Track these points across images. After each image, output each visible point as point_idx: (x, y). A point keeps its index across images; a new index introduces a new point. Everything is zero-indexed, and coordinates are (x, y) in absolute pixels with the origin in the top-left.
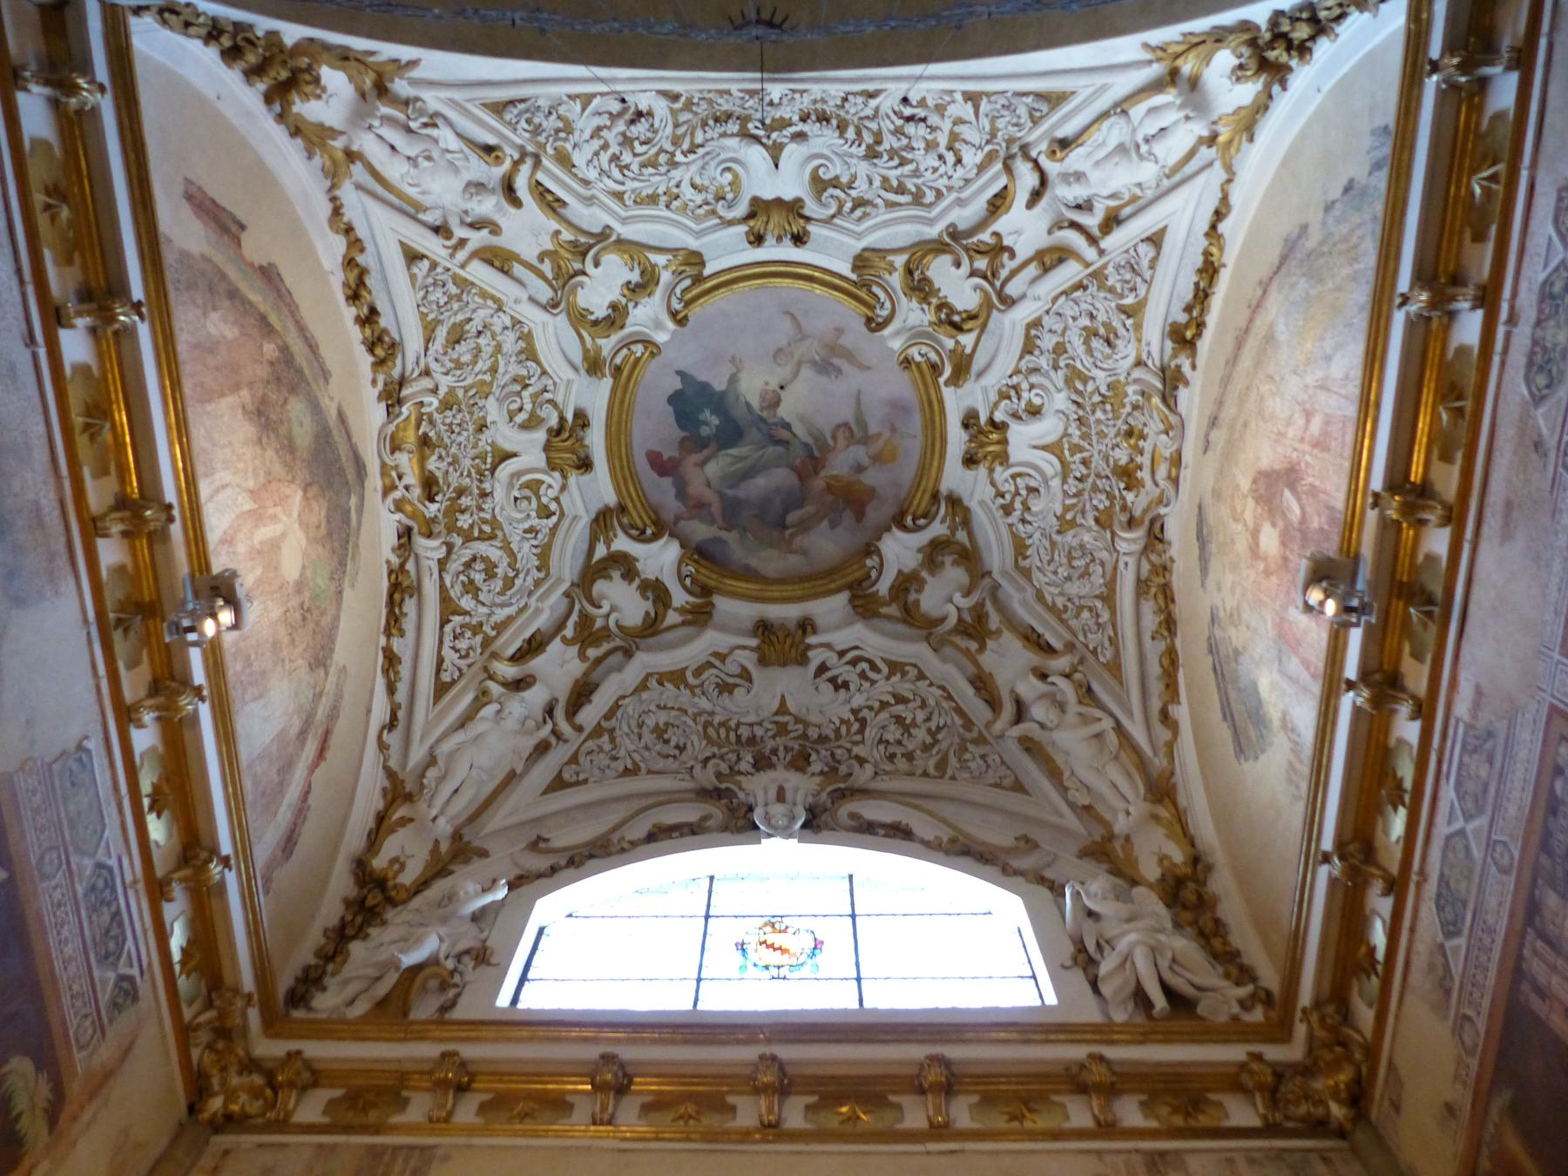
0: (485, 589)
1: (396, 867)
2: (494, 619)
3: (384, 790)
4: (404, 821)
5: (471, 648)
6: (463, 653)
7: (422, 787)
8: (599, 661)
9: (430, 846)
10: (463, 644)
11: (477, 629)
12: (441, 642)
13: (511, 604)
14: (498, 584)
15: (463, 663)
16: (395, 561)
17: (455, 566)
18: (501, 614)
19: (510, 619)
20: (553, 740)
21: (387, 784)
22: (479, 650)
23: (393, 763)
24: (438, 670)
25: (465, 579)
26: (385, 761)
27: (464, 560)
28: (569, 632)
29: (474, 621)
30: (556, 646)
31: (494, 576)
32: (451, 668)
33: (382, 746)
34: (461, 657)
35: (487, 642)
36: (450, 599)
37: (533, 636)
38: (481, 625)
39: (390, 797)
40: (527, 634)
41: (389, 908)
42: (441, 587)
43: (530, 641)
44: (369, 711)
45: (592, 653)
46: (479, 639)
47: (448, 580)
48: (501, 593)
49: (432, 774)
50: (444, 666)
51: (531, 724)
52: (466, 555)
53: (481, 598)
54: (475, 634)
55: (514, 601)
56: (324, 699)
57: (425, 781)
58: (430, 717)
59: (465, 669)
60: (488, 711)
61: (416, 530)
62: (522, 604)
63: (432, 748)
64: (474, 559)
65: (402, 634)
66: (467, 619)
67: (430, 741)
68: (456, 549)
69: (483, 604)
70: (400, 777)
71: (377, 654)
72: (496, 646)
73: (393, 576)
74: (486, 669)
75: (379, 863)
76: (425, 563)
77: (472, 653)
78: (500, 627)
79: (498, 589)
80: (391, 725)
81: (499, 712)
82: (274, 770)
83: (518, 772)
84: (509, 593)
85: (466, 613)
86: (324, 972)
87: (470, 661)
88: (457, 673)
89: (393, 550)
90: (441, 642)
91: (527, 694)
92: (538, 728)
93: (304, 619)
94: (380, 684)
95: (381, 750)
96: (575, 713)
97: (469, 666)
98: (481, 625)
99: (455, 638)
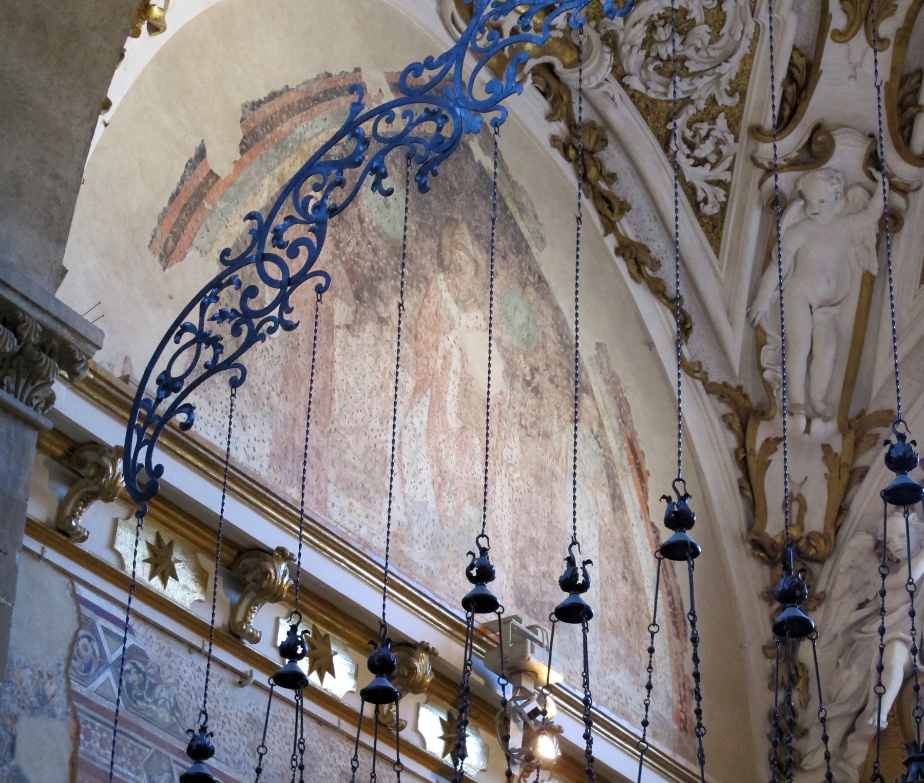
0: (690, 52)
1: (795, 507)
2: (725, 84)
3: (724, 417)
4: (771, 445)
5: (719, 142)
6: (713, 159)
7: (768, 387)
8: (904, 35)
9: (820, 454)
10: (705, 150)
11: (710, 114)
12: (677, 168)
13: (739, 42)
14: (702, 32)
15: (720, 173)
16: (559, 128)
17: (633, 60)
18: (730, 69)
19: (747, 61)
20: (898, 200)
21: (724, 408)
22: (731, 138)
23: (716, 377)
24: (696, 207)
25: (657, 63)
26: (704, 381)
27: (639, 42)
28: (839, 20)
29: (702, 105)
30: (833, 54)
31: (693, 23)
32: (707, 188)
33: (689, 368)
34: (713, 166)
35: (733, 126)
36: (654, 101)
37: (792, 64)
38: (712, 100)
39: (737, 425)
40: (781, 73)
41: (815, 567)
42: (632, 97)
43: (790, 78)
44: (650, 345)
45: (888, 28)
46: (721, 122)
47: (635, 83)
48: (716, 36)
49: (768, 355)
50: (700, 196)
51: (858, 194)
52: (639, 33)
53: (692, 67)
54: (713, 120)
55: (738, 36)
56: (606, 423)
57: (767, 375)
58: (722, 276)
59: (726, 177)
60: (792, 214)
61: (559, 67)
62: (751, 29)
63: (748, 315)
64: (652, 27)
65: (624, 208)
66: (691, 110)
67: (741, 319)
68: (621, 37)
69: (700, 74)
70: (733, 384)
71: (615, 267)
72: (749, 117)
73: (572, 153)
74: (753, 160)
75: (774, 527)
76: (596, 94)
77: (724, 149)
78: (738, 88)
79: (707, 38)
80: (684, 328)
81: (805, 206)
82: (621, 584)
83: (875, 272)
84: (724, 30)
85: (688, 101)
86: (794, 712)
87: (726, 163)
88: (721, 193)
89: (550, 118)
90: (677, 168)
91: (832, 163)
92: (871, 194)
93: (536, 391)
94: (640, 294)
95: (694, 377)
96: (908, 141)
97: (730, 169)
98: (712, 100)
99: (692, 146)
